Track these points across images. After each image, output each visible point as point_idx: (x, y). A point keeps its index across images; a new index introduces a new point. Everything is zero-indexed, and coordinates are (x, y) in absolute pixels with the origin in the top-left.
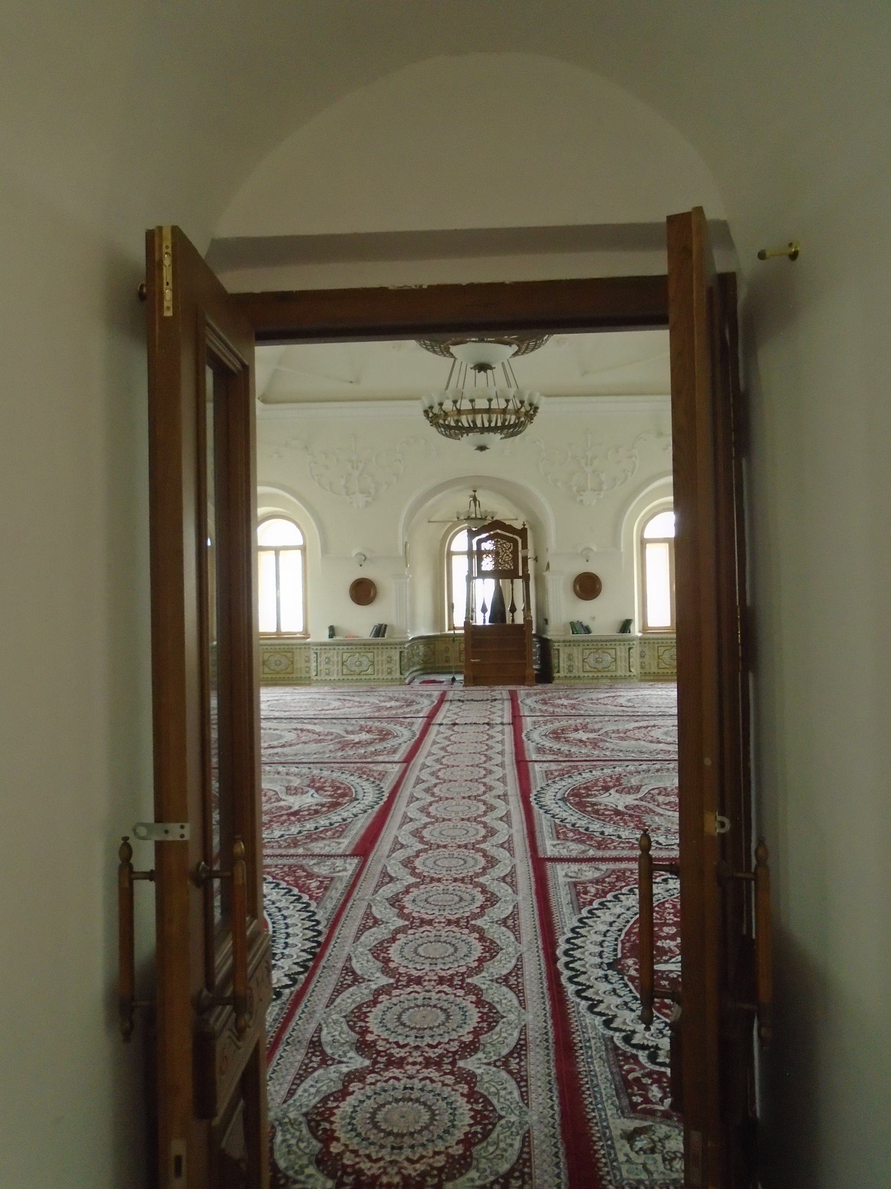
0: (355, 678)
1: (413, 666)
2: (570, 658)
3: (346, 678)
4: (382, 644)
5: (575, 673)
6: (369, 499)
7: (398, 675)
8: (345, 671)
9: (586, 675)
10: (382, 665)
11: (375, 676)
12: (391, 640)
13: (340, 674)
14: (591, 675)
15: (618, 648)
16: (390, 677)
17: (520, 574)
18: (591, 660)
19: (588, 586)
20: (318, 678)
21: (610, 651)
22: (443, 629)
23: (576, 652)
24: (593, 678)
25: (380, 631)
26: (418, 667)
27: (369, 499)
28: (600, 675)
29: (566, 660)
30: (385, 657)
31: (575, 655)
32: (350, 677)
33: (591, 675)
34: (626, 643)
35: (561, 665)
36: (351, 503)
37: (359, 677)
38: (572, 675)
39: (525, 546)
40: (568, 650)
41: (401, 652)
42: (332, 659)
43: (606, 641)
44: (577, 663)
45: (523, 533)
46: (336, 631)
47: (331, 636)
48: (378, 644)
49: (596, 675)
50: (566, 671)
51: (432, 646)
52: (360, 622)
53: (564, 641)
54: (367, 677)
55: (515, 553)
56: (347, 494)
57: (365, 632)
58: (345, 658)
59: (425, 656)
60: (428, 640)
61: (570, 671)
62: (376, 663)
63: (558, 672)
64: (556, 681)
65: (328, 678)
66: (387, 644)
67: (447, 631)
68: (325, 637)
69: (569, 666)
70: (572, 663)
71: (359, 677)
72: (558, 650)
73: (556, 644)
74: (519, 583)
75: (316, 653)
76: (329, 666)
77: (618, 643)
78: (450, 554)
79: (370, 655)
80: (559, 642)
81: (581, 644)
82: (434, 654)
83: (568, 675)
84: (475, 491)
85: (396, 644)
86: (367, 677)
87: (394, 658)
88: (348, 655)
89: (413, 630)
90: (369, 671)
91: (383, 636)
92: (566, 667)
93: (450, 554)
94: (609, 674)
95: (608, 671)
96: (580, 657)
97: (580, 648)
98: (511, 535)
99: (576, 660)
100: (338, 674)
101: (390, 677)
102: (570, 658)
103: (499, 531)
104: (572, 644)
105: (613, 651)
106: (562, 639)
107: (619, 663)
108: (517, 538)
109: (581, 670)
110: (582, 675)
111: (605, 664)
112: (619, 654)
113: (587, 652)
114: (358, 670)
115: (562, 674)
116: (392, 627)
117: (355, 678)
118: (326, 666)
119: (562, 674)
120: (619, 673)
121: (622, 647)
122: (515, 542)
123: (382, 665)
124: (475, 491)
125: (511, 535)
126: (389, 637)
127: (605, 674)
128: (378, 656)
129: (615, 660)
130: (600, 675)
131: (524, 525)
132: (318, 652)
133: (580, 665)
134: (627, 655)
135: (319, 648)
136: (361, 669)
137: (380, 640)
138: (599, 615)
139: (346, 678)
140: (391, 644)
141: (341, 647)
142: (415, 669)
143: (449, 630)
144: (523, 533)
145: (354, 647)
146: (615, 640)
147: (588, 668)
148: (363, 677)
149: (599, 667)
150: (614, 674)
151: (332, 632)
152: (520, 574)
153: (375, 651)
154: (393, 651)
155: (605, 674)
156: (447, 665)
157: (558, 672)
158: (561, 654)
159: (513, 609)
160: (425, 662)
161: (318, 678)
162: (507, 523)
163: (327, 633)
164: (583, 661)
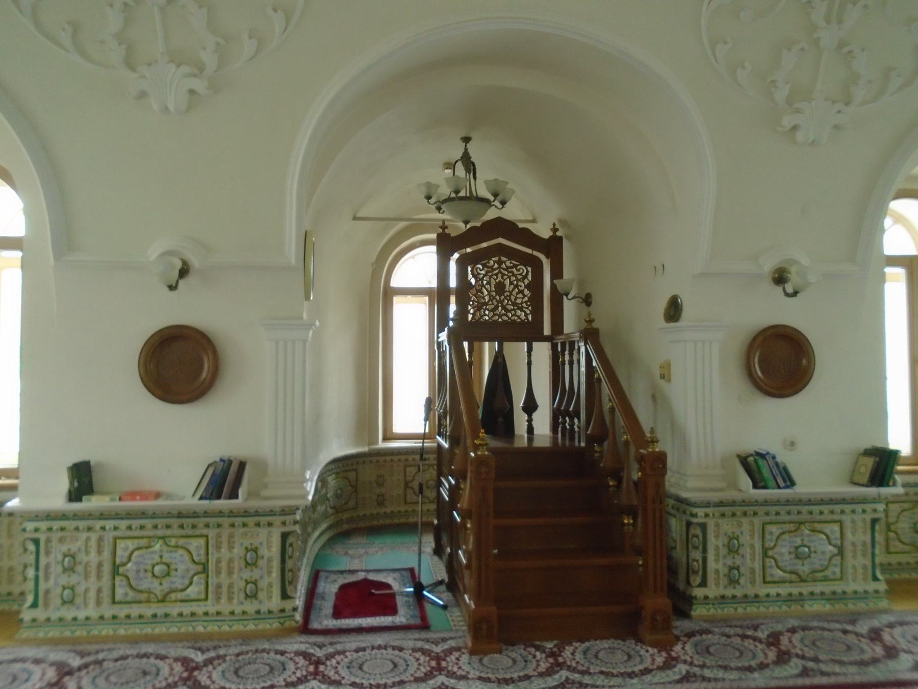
0: (148, 611)
1: (314, 529)
3: (122, 612)
4: (232, 514)
5: (744, 588)
6: (199, 85)
7: (275, 602)
8: (120, 592)
9: (773, 590)
10: (230, 573)
11: (210, 607)
12: (254, 504)
13: (106, 599)
14: (784, 590)
16: (250, 607)
17: (547, 331)
18: (783, 551)
19: (780, 362)
20: (40, 614)
21: (827, 528)
22: (373, 440)
23: (748, 532)
25: (224, 479)
26: (324, 526)
27: (199, 85)
28: (805, 589)
29: (723, 551)
30: (238, 551)
31: (745, 539)
32: (135, 611)
33: (784, 590)
35: (712, 565)
36: (143, 95)
37: (160, 610)
38: (739, 592)
39: (557, 273)
40: (727, 526)
41: (285, 536)
42: (82, 557)
43: (822, 502)
44: (750, 561)
45: (553, 247)
46: (96, 478)
47: (75, 496)
48: (220, 514)
49: (795, 591)
50: (724, 581)
51: (352, 475)
52: (168, 450)
53: (720, 504)
54: (187, 609)
55: (536, 286)
56: (130, 66)
57: (183, 484)
58: (121, 555)
59: (337, 496)
60: (343, 466)
61: (733, 582)
62: (211, 567)
63: (704, 584)
64: (698, 611)
65: (69, 613)
66: (246, 514)
67: (382, 445)
68: (54, 493)
69: (731, 569)
70: (738, 561)
71: (160, 610)
72: (703, 527)
73: (700, 512)
74: (542, 350)
75: (36, 542)
76: (74, 579)
77: (847, 508)
78: (390, 293)
79: (195, 544)
80: (708, 505)
81: (761, 510)
82: (355, 489)
83: (729, 592)
84: (467, 140)
85: (272, 513)
86: (187, 609)
87: (263, 551)
88: (131, 545)
89: (313, 437)
90: (193, 591)
91: (234, 495)
92: (724, 570)
93: (390, 293)
94: (827, 588)
95: (826, 579)
97: (757, 521)
98: (529, 251)
99: (747, 551)
100: (98, 603)
101: (250, 607)
102: (733, 549)
103: (501, 240)
104: (739, 510)
105: (836, 527)
106: (715, 497)
107: (848, 554)
108: (542, 257)
110: (763, 591)
111: (817, 561)
112: (849, 535)
113: (775, 529)
114: (158, 589)
115: (712, 591)
116: (262, 466)
117: (148, 611)
118: (64, 580)
119: (712, 591)
122: (537, 267)
123: (230, 573)
124: (467, 140)
125: (529, 251)
126: (250, 495)
128: (218, 548)
129: (841, 551)
130: (805, 589)
131: (555, 230)
132: (43, 538)
133: (757, 566)
134: (868, 539)
135: (43, 525)
136: (166, 586)
137: (222, 504)
138: (805, 435)
139: (122, 612)
140: (257, 514)
141: (109, 524)
142: (317, 533)
143: (385, 439)
144: (553, 247)
145: (148, 523)
146: (843, 501)
148: (174, 610)
149: (804, 568)
150: (838, 587)
151: (83, 479)
152: (547, 331)
153: (212, 533)
154: (263, 532)
155: (818, 588)
156: (382, 510)
157: (704, 584)
158: (712, 541)
159: (530, 406)
160: (337, 510)
161: (40, 614)
162: (521, 225)
163: (63, 484)
164: (765, 554)
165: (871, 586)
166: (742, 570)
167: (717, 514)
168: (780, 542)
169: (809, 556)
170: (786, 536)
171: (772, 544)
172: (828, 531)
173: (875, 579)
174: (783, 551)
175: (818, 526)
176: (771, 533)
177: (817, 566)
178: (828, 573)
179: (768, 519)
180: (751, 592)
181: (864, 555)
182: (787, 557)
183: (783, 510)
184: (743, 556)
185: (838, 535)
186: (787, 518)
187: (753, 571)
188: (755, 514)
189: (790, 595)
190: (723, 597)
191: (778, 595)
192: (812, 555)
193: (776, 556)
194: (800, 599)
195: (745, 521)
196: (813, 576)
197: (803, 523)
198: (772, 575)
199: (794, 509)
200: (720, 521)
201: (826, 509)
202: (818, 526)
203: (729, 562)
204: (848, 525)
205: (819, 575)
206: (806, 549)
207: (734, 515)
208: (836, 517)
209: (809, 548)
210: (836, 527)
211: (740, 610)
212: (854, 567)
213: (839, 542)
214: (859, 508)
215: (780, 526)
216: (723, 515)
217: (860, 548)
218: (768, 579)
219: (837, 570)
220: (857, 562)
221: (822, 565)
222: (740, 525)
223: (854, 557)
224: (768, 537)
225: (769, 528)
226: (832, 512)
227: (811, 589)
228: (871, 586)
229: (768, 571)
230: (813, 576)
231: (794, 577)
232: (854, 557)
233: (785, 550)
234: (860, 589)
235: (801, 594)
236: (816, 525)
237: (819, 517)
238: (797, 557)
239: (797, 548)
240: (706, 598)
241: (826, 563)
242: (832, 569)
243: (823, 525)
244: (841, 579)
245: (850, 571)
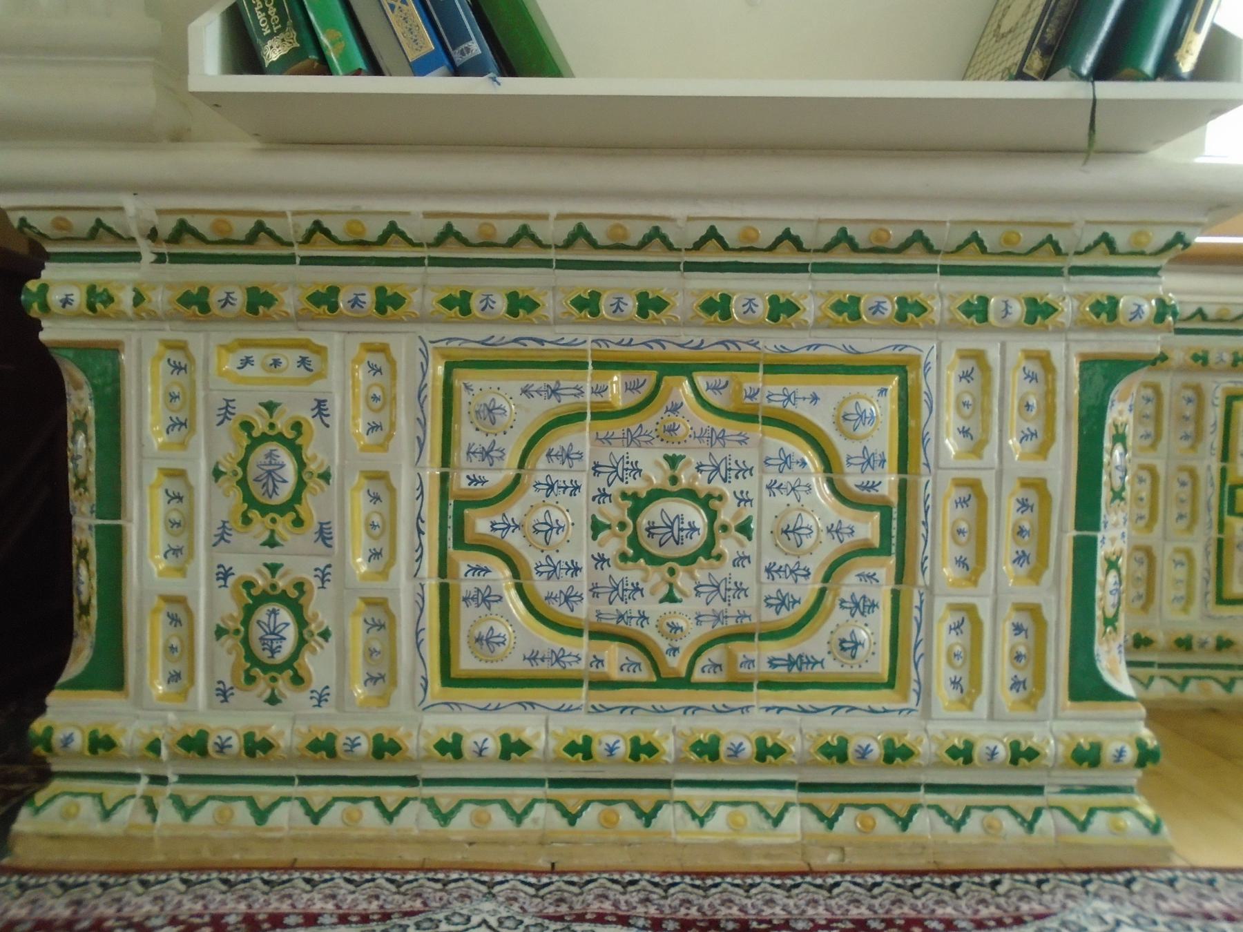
2: (268, 479)
5: (341, 696)
9: (481, 724)
14: (543, 726)
15: (941, 361)
18: (564, 520)
21: (819, 402)
23: (360, 402)
24: (580, 773)
28: (671, 727)
29: (211, 504)
33: (543, 726)
34: (1068, 295)
35: (147, 564)
38: (287, 726)
40: (226, 365)
44: (370, 551)
49: (611, 731)
50: (212, 660)
53: (179, 240)
69: (256, 599)
70: (299, 561)
77: (942, 294)
80: (103, 241)
81: (422, 287)
83: (229, 725)
92: (210, 604)
94: (800, 727)
95: (795, 679)
96: (413, 476)
104: (291, 284)
105: (878, 402)
109: (415, 657)
110: (422, 725)
111: (751, 580)
113: (516, 402)
120: (939, 722)
121: (1006, 351)
127: (741, 726)
129: (897, 534)
130: (671, 727)
133: (410, 587)
147: (515, 631)
149: (681, 617)
150: (866, 728)
155: (741, 726)
157: (110, 673)
164: (456, 534)
165: (1057, 727)
166: (320, 608)
167: (159, 299)
168: (542, 468)
169: (708, 549)
170: (581, 438)
171: (496, 479)
172: (821, 418)
173: (1088, 686)
174: (564, 520)
175: (770, 391)
176: (489, 413)
177: (751, 608)
178: (815, 644)
179: (469, 336)
180: (356, 730)
181: (1032, 561)
182: (578, 547)
183: (553, 288)
184: (324, 535)
185: (884, 440)
186: (585, 337)
187: (380, 616)
188: (388, 302)
189: (582, 749)
190: (195, 745)
191: (512, 748)
192: (728, 545)
193: (514, 540)
194: (640, 776)
195: (339, 344)
196: (729, 660)
197: (686, 369)
198: (485, 642)
199: (621, 287)
200: (203, 341)
201: (811, 293)
202: (770, 391)
203: (248, 563)
204: (944, 382)
205: (761, 654)
206: (698, 517)
207: (259, 302)
208: (871, 343)
209: (707, 502)
210: (878, 402)
211: (286, 817)
212: (968, 617)
213: (887, 483)
214: (1008, 295)
215: (541, 379)
216: (196, 303)
217: (1006, 514)
218: (466, 662)
219: (873, 632)
220: (984, 587)
221: (783, 602)
222: (311, 361)
223: (972, 567)
224: (467, 434)
225: (477, 388)
226: (849, 309)
227: (704, 726)
228: (1057, 727)
229: (467, 618)
230: (729, 660)
231: (614, 657)
232: (972, 567)
233: (573, 513)
234: (994, 738)
235: (642, 750)
236: (754, 381)
237: (772, 341)
238: (637, 552)
239: (638, 504)
240: (101, 744)
241: (806, 591)
242: (837, 620)
243: (802, 386)
244: (890, 685)
245: (944, 639)
